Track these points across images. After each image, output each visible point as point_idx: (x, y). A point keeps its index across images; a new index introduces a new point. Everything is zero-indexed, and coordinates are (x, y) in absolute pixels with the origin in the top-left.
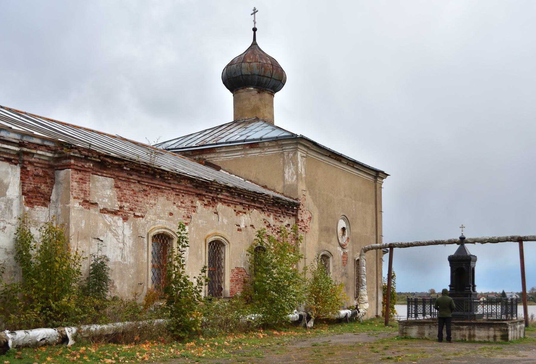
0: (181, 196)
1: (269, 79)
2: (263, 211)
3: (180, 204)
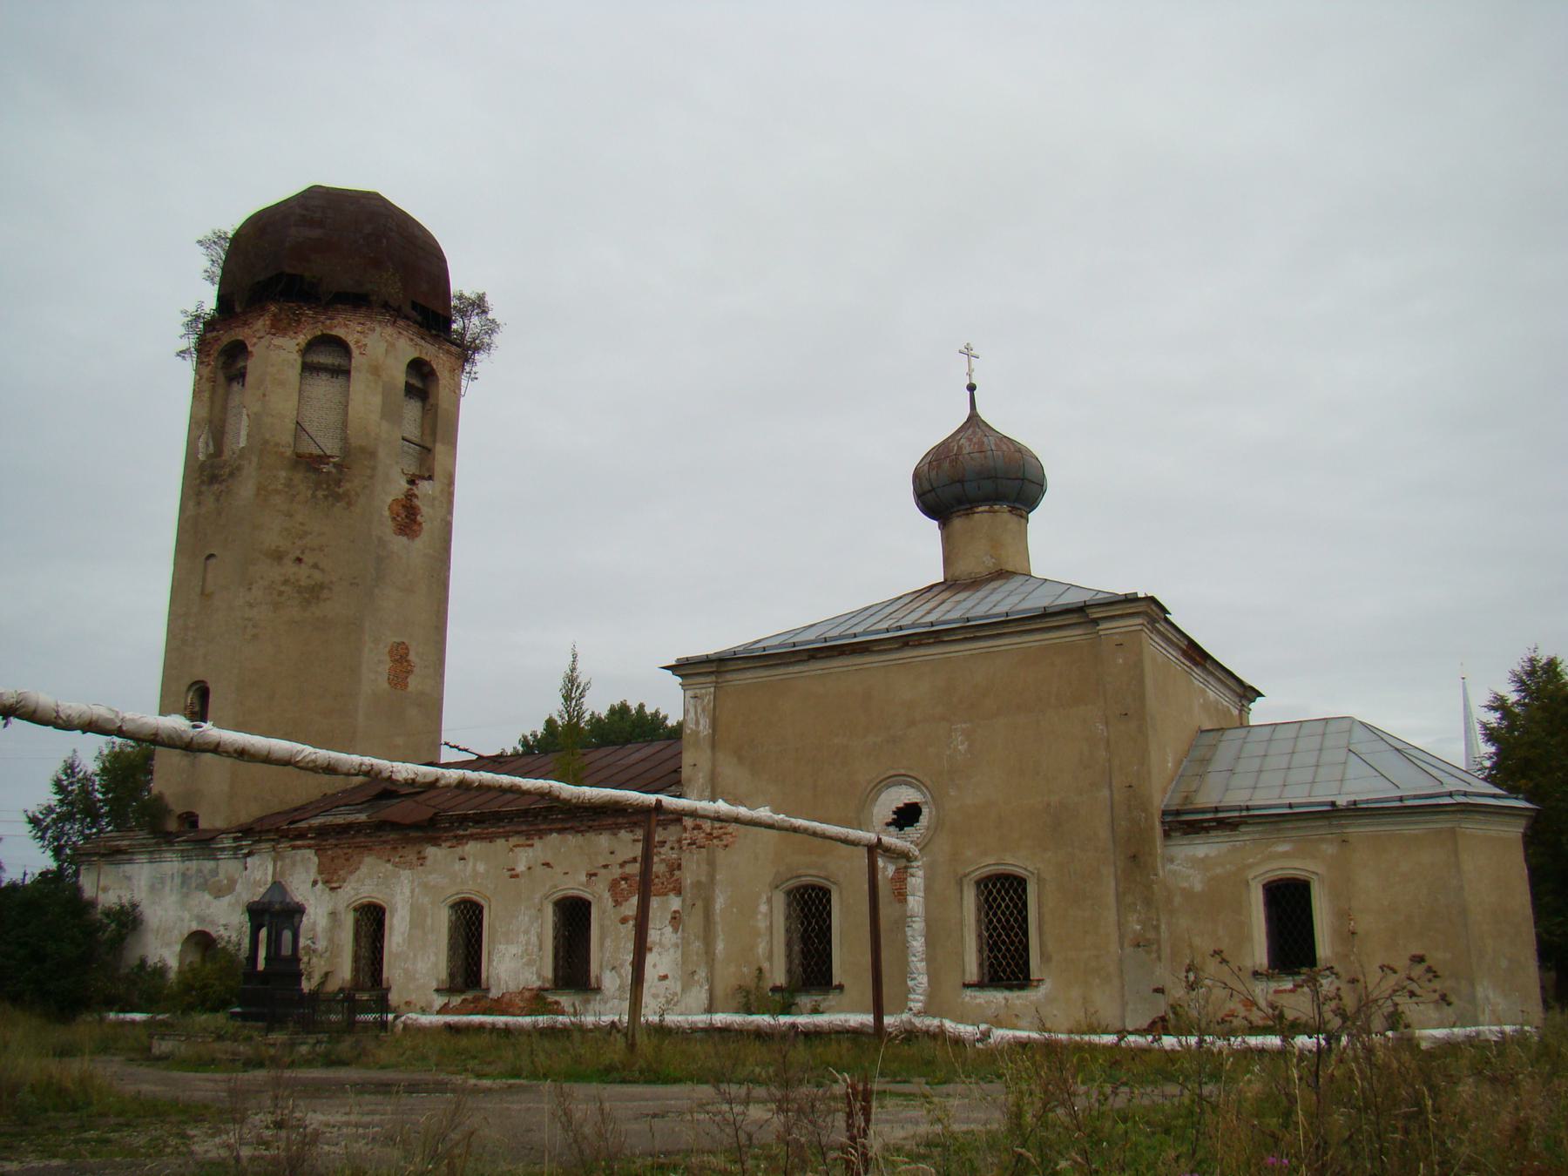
0: (400, 849)
1: (933, 493)
2: (578, 832)
3: (397, 860)
